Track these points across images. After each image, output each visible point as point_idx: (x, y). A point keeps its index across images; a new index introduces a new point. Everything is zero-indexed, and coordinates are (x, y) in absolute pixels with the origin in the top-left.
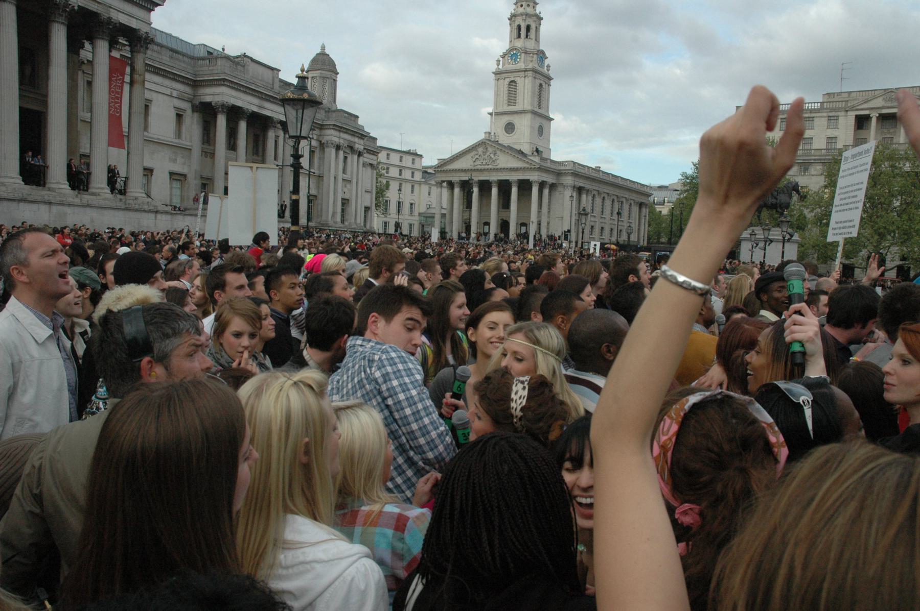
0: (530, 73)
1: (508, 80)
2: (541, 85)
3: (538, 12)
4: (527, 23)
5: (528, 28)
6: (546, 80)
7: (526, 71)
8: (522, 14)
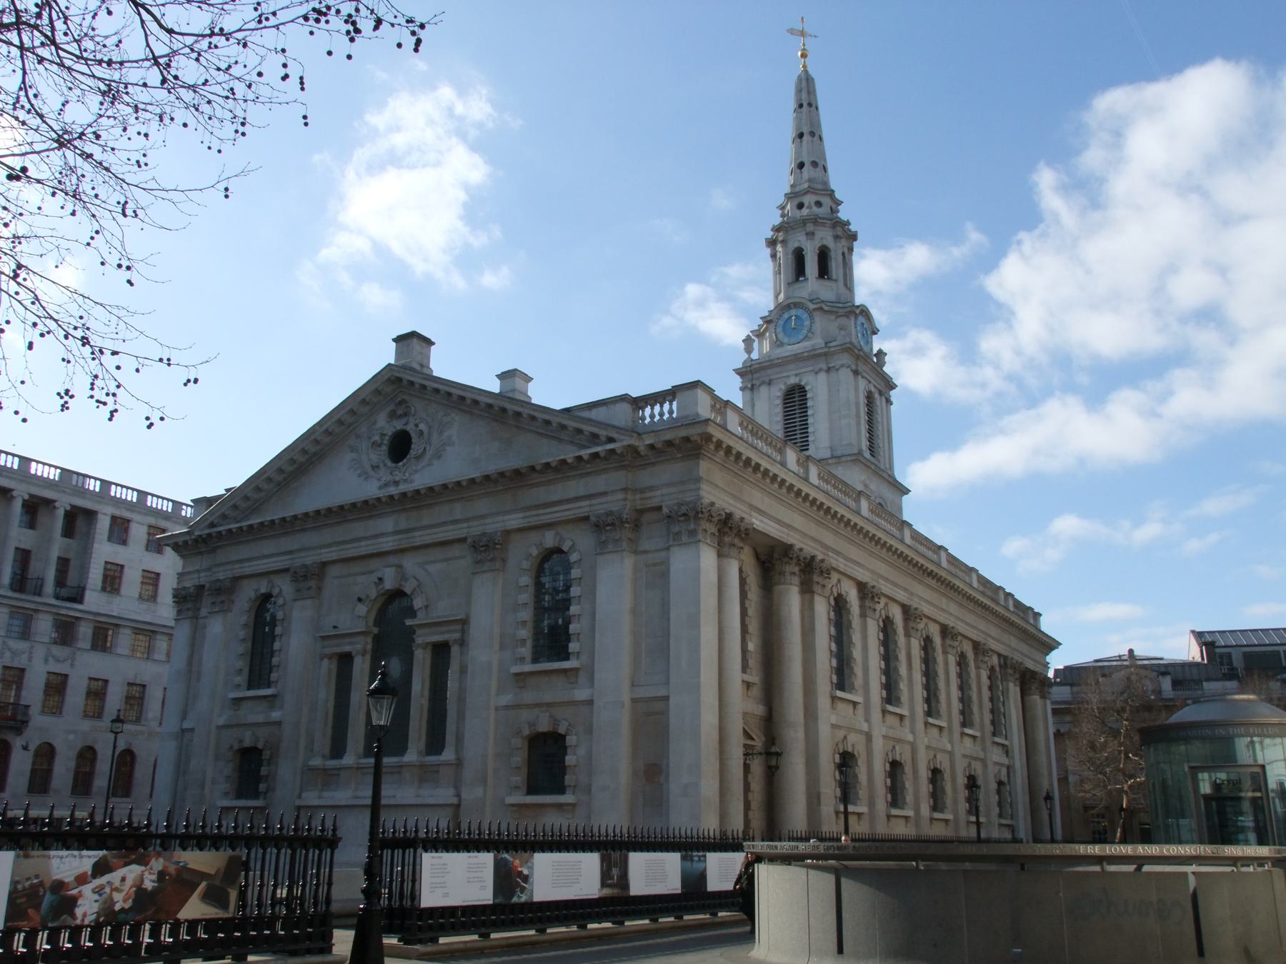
2: (869, 397)
3: (843, 214)
5: (823, 256)
8: (804, 222)
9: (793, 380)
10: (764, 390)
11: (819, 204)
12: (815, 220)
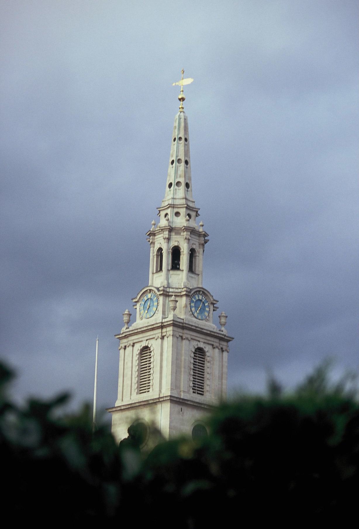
0: (169, 330)
1: (138, 347)
2: (200, 351)
4: (173, 243)
5: (176, 252)
6: (216, 342)
7: (162, 327)
8: (162, 230)
9: (144, 344)
10: (131, 348)
11: (177, 214)
12: (171, 230)
